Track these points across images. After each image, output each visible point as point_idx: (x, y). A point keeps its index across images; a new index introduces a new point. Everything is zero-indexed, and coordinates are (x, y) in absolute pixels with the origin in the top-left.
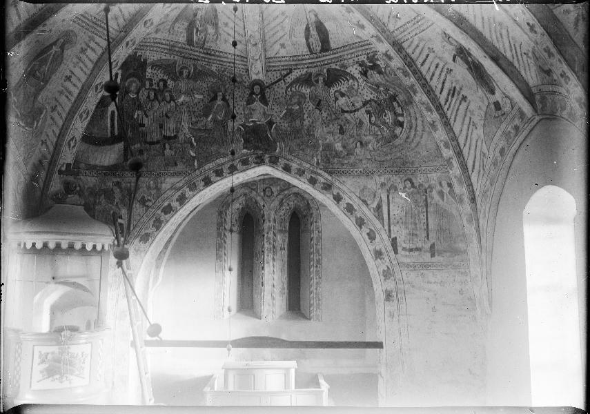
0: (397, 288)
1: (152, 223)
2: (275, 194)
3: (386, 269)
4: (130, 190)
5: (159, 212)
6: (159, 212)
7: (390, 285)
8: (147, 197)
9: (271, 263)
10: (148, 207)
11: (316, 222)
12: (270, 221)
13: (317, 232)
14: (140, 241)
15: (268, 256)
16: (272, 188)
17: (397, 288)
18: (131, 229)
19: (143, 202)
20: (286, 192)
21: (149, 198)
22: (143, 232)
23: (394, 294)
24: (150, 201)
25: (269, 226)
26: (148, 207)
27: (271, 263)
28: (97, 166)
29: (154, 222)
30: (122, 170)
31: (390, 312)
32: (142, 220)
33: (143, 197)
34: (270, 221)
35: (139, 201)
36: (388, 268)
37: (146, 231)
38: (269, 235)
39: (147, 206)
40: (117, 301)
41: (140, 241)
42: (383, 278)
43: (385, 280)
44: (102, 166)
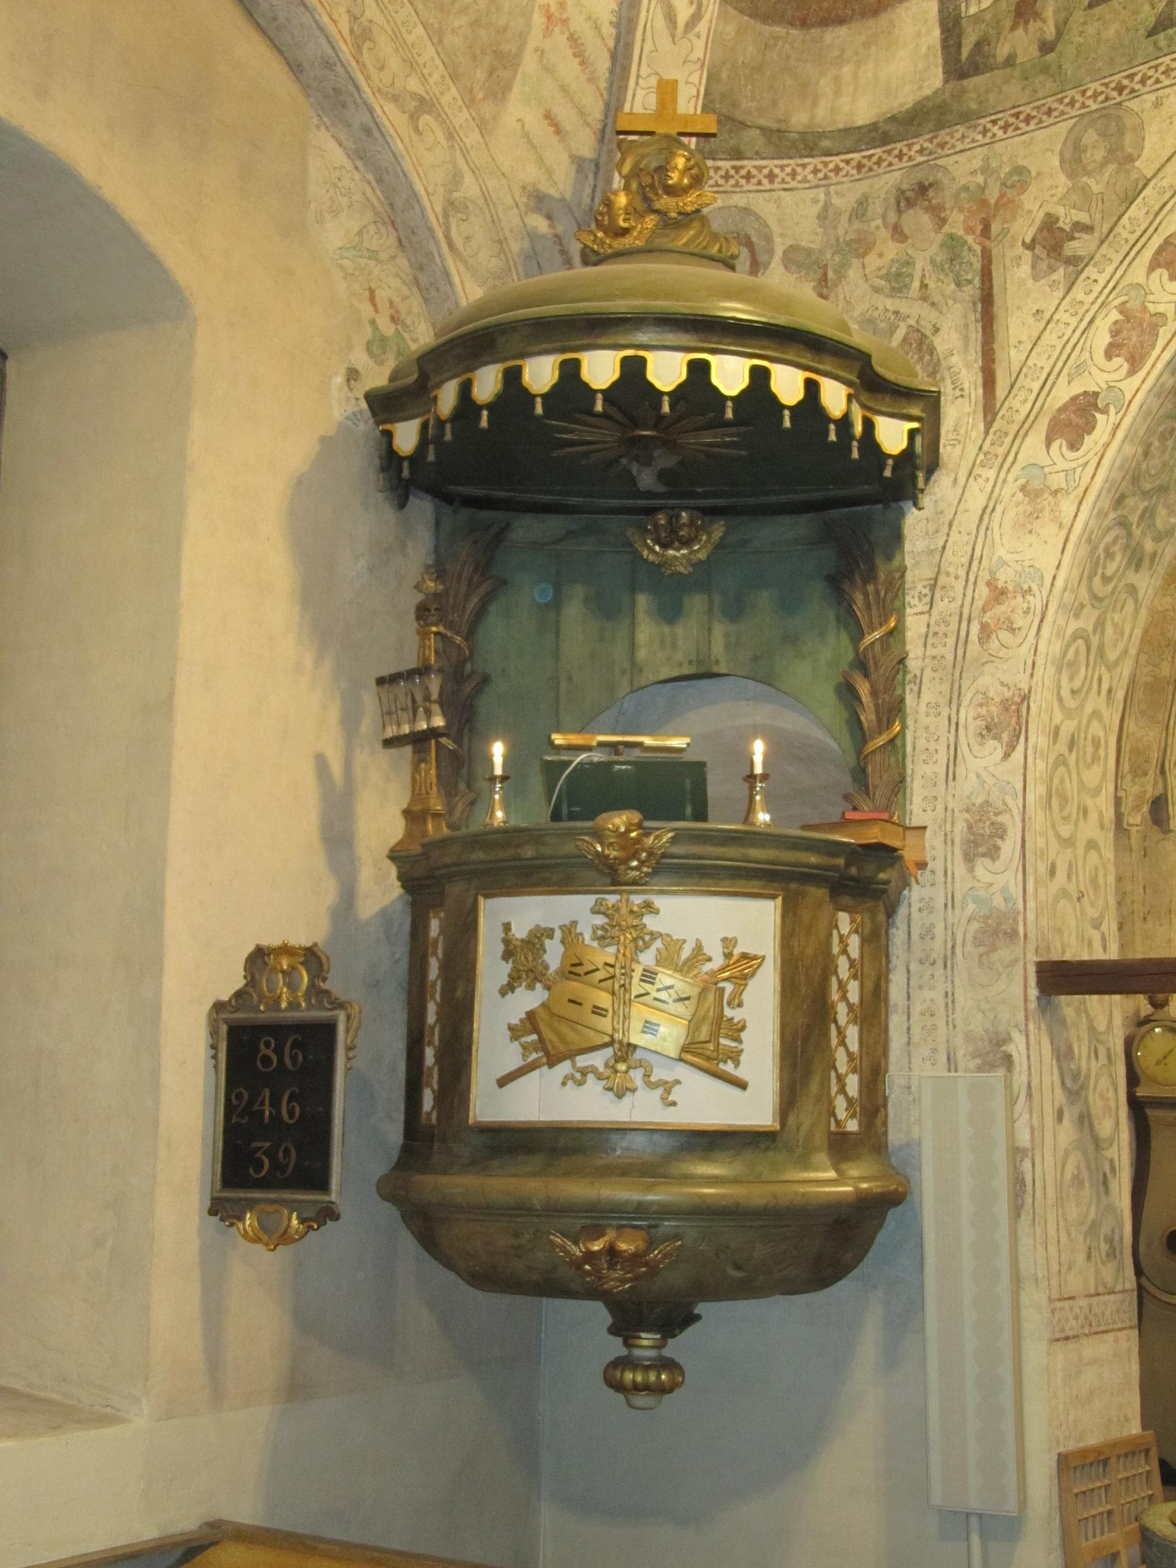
1: (1101, 337)
4: (984, 203)
5: (1138, 273)
6: (1138, 273)
8: (1067, 218)
10: (1075, 262)
14: (1049, 442)
18: (1000, 393)
19: (1052, 242)
21: (1083, 217)
22: (1063, 393)
24: (1088, 229)
26: (1075, 262)
28: (822, 135)
29: (1115, 333)
30: (940, 125)
32: (1050, 338)
33: (1049, 224)
35: (1030, 247)
37: (1077, 389)
39: (1073, 261)
40: (954, 757)
41: (1049, 442)
44: (847, 131)
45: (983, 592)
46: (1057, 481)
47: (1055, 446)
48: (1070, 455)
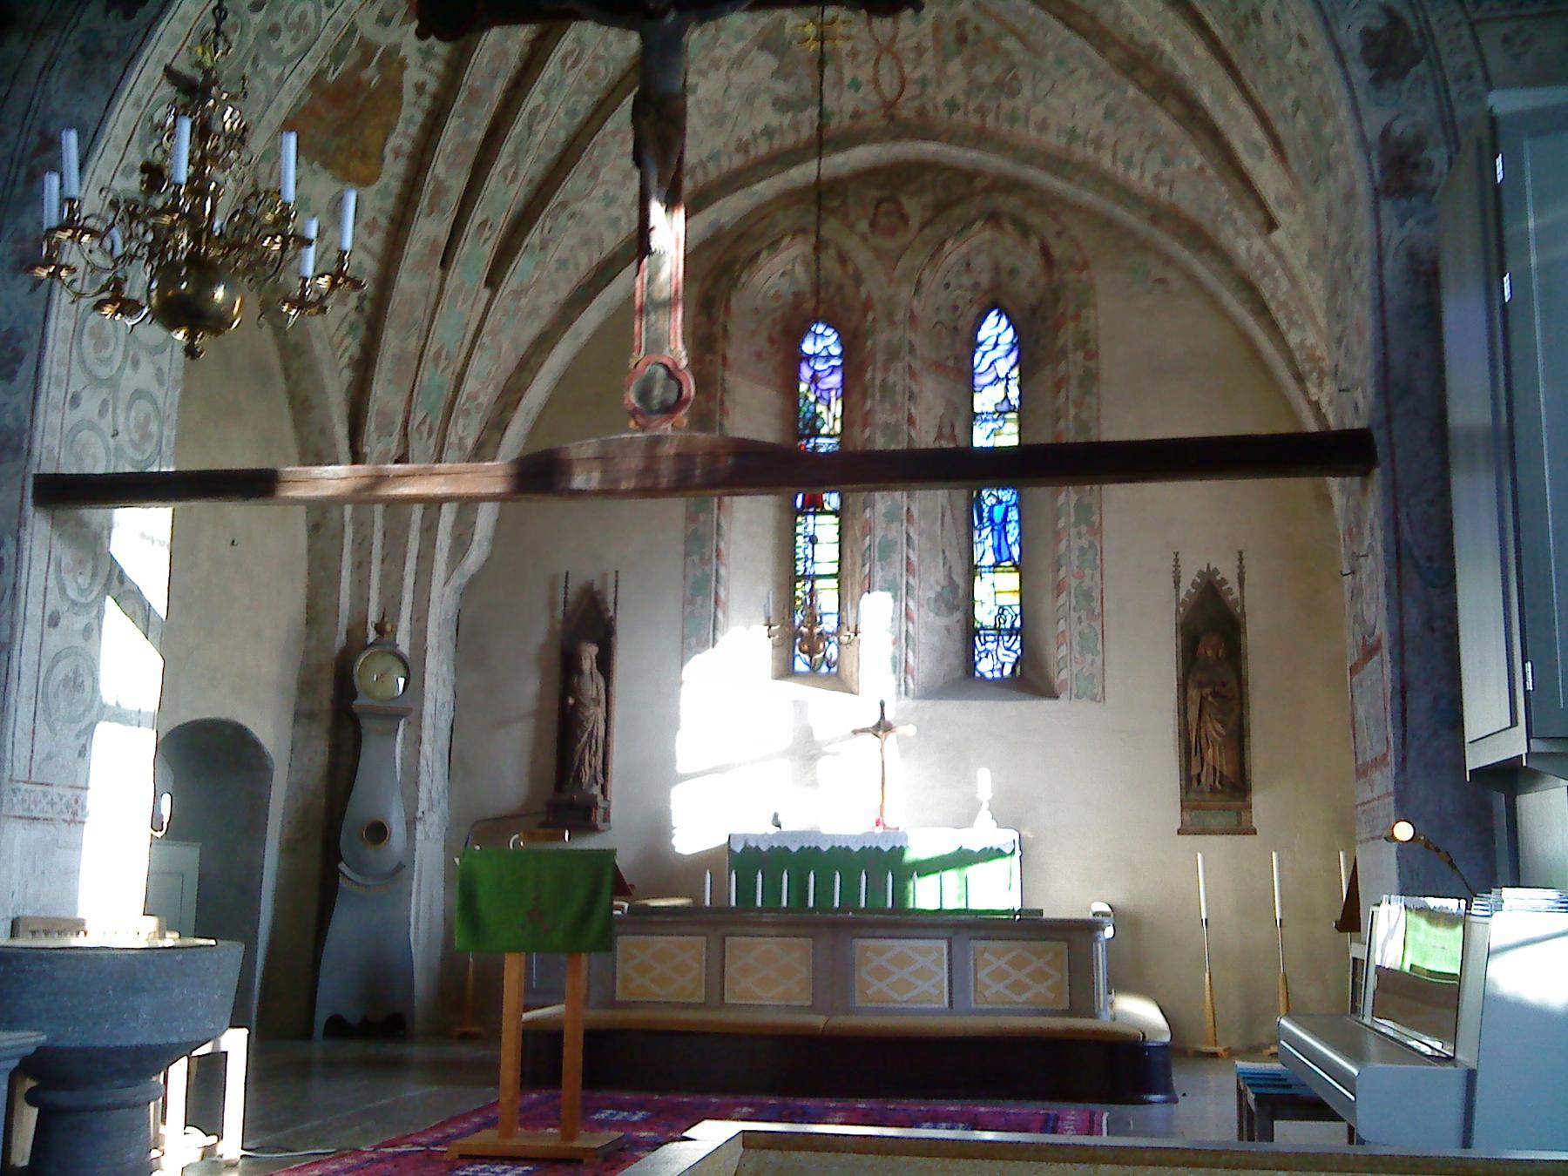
0: (1449, 124)
2: (915, 222)
3: (1379, 24)
7: (1409, 110)
11: (1077, 317)
12: (892, 323)
13: (1080, 355)
16: (904, 199)
17: (1449, 124)
20: (957, 212)
23: (1437, 154)
31: (1412, 255)
34: (892, 323)
36: (1394, 19)
38: (892, 378)
41: (107, 11)
42: (1360, 73)
43: (1377, 82)
45: (34, 139)
46: (110, 45)
47: (112, 14)
48: (124, 24)
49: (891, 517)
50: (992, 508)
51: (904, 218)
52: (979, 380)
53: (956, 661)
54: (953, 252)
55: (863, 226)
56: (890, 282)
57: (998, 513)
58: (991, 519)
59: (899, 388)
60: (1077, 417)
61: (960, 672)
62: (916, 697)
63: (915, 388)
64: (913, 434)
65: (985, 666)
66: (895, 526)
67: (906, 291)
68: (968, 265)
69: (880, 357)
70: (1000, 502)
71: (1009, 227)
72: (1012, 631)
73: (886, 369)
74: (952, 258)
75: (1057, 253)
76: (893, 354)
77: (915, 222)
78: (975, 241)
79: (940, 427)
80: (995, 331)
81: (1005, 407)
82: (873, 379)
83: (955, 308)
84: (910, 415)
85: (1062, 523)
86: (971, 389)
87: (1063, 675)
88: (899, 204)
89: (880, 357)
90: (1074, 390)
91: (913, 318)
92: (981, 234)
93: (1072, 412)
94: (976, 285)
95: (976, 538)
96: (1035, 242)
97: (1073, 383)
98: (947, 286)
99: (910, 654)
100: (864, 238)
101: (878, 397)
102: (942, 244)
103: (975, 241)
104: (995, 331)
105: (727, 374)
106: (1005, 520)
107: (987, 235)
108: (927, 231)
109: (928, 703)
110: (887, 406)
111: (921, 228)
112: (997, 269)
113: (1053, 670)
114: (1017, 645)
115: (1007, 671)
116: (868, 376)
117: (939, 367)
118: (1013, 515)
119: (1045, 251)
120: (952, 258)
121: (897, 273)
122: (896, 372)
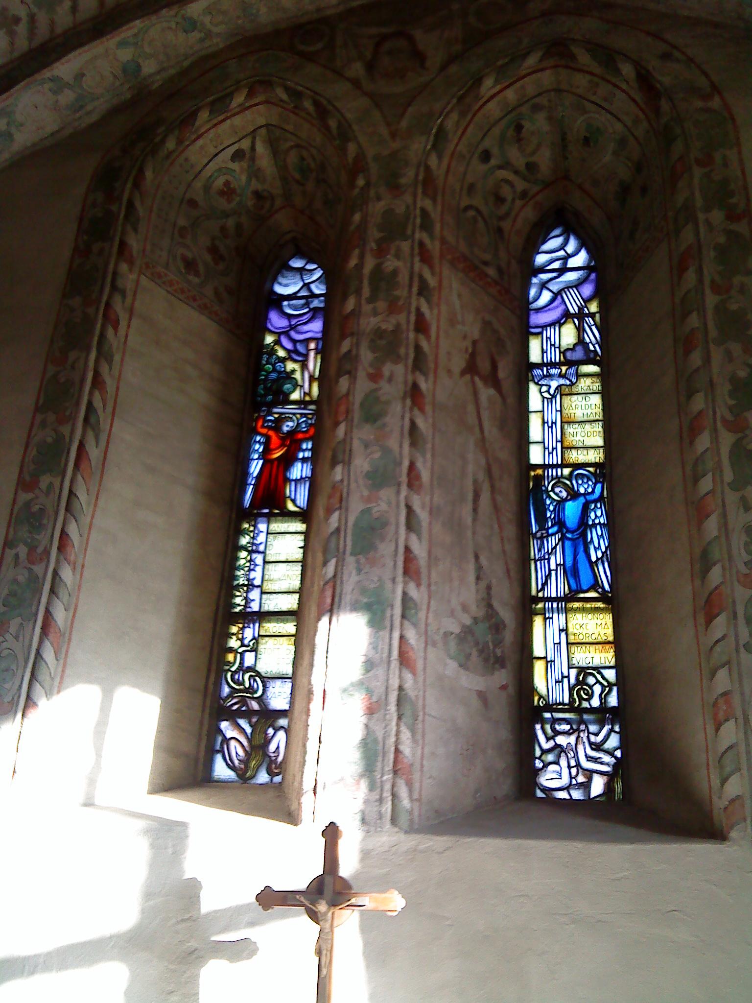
2: (435, 59)
9: (396, 416)
12: (395, 188)
13: (717, 216)
15: (375, 377)
25: (388, 213)
27: (396, 416)
49: (379, 479)
50: (562, 502)
51: (419, 57)
52: (537, 319)
53: (499, 762)
54: (497, 97)
55: (357, 69)
56: (393, 135)
57: (572, 510)
58: (560, 523)
59: (403, 277)
60: (720, 309)
61: (506, 786)
62: (412, 829)
63: (432, 282)
64: (424, 344)
65: (554, 778)
66: (387, 494)
67: (418, 145)
68: (519, 128)
69: (374, 234)
70: (574, 495)
71: (584, 58)
72: (603, 714)
73: (381, 253)
74: (493, 109)
75: (664, 78)
76: (394, 229)
77: (435, 59)
78: (530, 86)
79: (473, 356)
80: (563, 259)
81: (579, 354)
82: (360, 266)
83: (500, 200)
84: (420, 315)
85: (706, 484)
86: (525, 332)
87: (734, 787)
88: (411, 39)
89: (374, 234)
90: (710, 269)
91: (428, 183)
92: (537, 78)
93: (711, 300)
94: (531, 167)
95: (534, 552)
96: (627, 69)
97: (710, 255)
98: (486, 156)
99: (406, 735)
100: (356, 83)
101: (366, 291)
102: (478, 81)
103: (530, 86)
104: (563, 259)
105: (124, 267)
106: (584, 524)
107: (547, 78)
108: (453, 69)
109: (439, 842)
110: (381, 305)
111: (444, 67)
112: (562, 143)
113: (705, 779)
114: (613, 741)
115: (598, 786)
116: (353, 262)
117: (471, 269)
118: (598, 515)
119: (645, 80)
120: (493, 109)
121: (404, 124)
122: (397, 256)
